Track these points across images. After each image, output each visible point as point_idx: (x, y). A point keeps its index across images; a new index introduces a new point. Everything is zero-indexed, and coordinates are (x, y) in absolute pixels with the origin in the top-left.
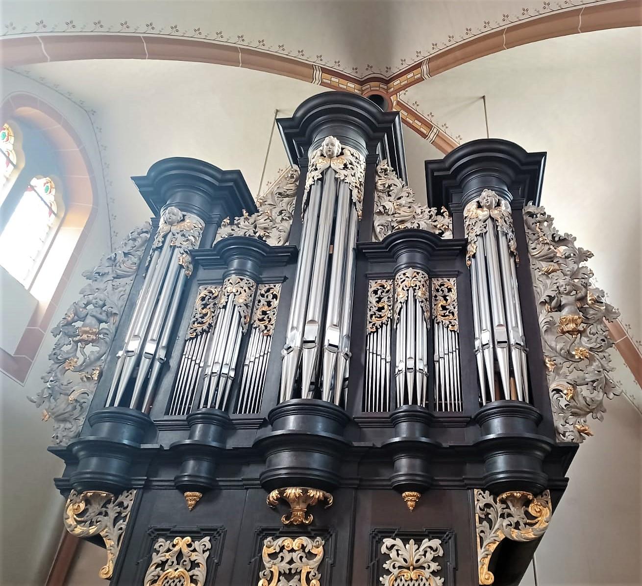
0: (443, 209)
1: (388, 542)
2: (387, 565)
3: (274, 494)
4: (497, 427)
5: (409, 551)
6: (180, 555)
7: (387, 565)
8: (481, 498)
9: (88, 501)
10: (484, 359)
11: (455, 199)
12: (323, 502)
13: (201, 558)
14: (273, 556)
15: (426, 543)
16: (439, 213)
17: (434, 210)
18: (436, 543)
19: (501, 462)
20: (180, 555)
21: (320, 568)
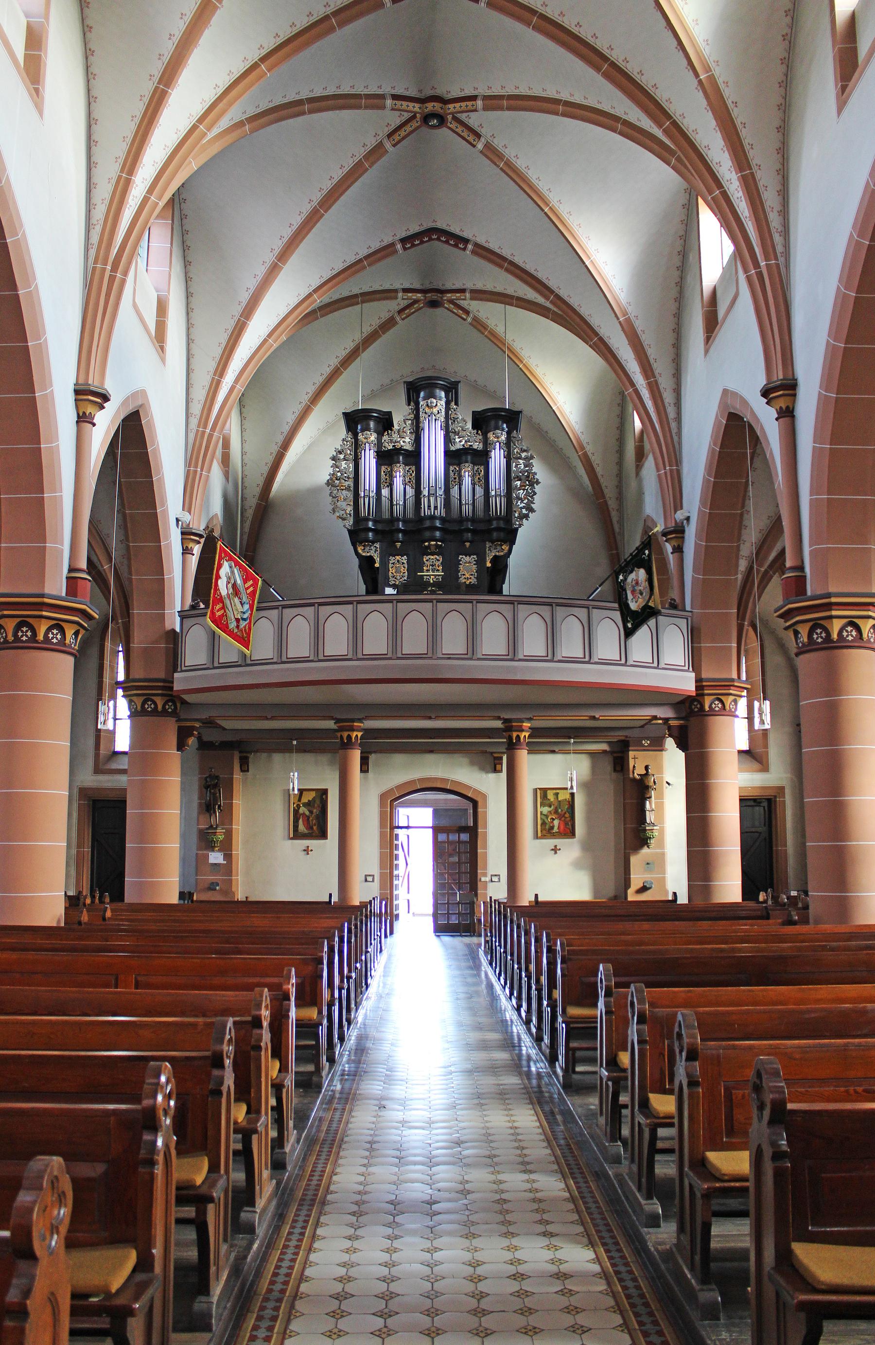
0: (480, 432)
1: (461, 556)
2: (461, 562)
3: (426, 544)
4: (495, 524)
5: (468, 559)
6: (398, 561)
7: (461, 562)
8: (488, 545)
9: (364, 546)
10: (492, 501)
11: (484, 427)
12: (441, 545)
13: (405, 562)
14: (427, 560)
15: (472, 557)
16: (477, 433)
17: (475, 431)
18: (475, 556)
19: (495, 534)
20: (398, 561)
21: (441, 563)
